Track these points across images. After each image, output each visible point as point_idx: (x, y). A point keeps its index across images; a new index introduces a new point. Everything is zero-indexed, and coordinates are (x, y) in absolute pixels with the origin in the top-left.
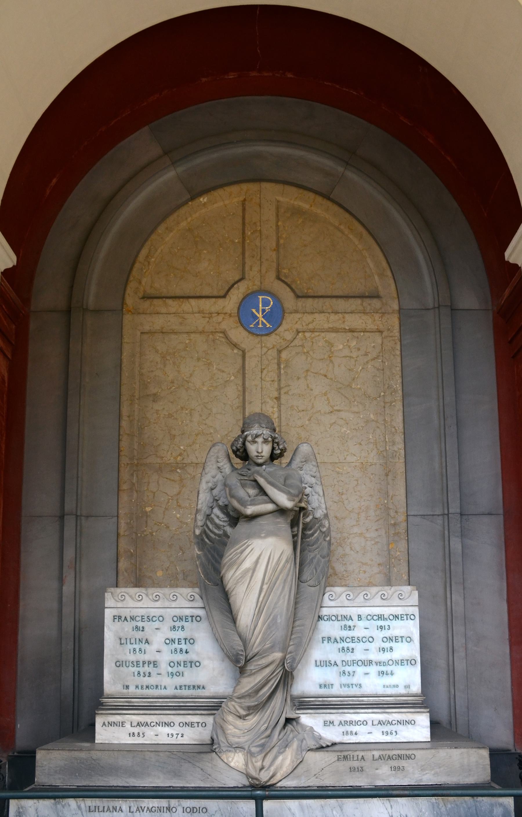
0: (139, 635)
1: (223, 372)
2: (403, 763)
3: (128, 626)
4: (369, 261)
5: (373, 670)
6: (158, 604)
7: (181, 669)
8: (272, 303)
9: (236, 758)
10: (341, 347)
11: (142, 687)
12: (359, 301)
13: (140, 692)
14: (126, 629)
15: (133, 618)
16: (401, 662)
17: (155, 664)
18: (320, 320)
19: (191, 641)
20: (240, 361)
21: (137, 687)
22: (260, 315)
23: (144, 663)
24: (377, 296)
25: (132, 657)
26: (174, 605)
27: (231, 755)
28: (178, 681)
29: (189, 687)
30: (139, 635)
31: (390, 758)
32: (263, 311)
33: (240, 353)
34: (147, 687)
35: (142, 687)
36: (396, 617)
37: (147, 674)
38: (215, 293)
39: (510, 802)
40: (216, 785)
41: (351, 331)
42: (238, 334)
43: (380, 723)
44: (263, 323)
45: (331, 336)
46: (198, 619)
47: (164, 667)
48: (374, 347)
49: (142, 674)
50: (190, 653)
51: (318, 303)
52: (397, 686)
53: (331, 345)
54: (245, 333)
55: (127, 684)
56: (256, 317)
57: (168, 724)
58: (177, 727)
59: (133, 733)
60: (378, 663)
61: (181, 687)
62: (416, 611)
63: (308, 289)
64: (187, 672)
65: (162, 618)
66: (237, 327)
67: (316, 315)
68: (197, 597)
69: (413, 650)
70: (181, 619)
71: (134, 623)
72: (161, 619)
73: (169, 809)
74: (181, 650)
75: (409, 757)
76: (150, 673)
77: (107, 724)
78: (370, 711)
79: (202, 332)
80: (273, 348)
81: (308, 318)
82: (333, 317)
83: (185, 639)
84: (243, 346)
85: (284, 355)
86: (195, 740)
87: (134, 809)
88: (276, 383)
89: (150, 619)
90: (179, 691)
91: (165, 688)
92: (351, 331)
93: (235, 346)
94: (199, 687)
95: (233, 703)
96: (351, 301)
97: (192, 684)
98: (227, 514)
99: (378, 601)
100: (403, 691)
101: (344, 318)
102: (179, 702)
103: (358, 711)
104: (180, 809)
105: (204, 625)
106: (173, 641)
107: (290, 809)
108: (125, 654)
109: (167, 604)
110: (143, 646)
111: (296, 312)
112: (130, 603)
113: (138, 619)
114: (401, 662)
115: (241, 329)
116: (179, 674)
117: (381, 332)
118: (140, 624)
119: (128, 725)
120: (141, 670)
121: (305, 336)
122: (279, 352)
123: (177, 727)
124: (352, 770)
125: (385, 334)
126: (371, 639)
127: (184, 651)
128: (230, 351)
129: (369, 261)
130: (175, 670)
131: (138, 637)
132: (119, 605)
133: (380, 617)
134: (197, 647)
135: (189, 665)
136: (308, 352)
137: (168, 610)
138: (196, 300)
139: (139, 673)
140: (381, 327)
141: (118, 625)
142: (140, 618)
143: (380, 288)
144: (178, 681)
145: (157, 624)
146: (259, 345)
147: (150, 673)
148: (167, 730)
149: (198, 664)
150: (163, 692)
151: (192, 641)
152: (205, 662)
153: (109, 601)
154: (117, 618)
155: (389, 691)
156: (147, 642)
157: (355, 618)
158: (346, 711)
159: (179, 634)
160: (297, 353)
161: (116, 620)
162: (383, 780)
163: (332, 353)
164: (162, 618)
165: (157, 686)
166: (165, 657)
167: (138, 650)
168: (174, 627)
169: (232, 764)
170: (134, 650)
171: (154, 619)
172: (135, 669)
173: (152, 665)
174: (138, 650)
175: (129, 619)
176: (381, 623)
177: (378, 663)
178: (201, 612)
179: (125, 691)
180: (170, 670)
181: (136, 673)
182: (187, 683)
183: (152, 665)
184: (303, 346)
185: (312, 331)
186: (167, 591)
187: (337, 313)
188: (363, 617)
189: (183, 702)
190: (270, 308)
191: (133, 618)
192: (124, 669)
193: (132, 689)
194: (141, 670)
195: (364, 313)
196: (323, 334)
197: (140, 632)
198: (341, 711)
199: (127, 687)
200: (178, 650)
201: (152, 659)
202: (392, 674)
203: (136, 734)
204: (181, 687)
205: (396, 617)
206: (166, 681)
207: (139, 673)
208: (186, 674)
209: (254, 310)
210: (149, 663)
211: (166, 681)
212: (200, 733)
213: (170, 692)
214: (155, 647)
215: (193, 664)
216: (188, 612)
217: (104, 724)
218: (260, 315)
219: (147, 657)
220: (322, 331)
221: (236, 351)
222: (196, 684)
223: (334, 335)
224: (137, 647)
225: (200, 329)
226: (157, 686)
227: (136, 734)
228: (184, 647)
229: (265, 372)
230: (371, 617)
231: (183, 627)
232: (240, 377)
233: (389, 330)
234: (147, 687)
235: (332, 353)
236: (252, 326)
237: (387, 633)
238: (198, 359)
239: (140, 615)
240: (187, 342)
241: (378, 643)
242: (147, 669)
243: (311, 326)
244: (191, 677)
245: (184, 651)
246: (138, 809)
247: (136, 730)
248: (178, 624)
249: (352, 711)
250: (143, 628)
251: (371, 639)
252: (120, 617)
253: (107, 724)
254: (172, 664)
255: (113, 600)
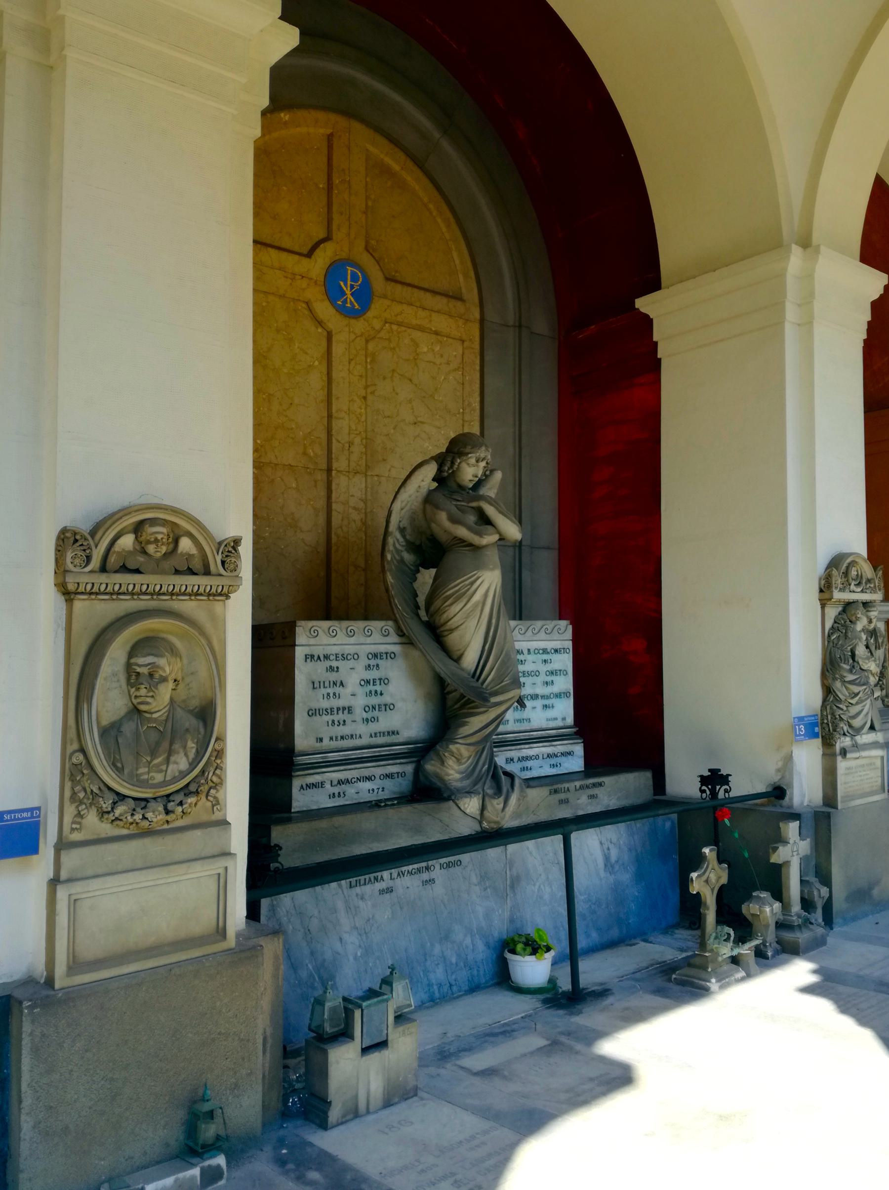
0: (333, 677)
1: (306, 353)
2: (596, 791)
3: (322, 666)
4: (455, 254)
5: (539, 703)
6: (352, 640)
7: (376, 713)
8: (361, 280)
9: (471, 804)
10: (425, 349)
11: (336, 738)
12: (445, 300)
13: (334, 744)
14: (319, 671)
15: (327, 657)
16: (558, 696)
17: (350, 710)
18: (409, 314)
19: (384, 681)
20: (324, 343)
21: (331, 738)
22: (348, 292)
23: (338, 709)
24: (458, 298)
25: (325, 704)
26: (369, 640)
27: (467, 800)
28: (374, 727)
29: (384, 733)
30: (333, 677)
31: (588, 787)
32: (352, 287)
33: (325, 333)
34: (342, 738)
35: (336, 738)
36: (556, 651)
37: (342, 723)
38: (297, 249)
39: (675, 816)
40: (454, 835)
41: (437, 333)
42: (324, 309)
43: (549, 756)
44: (351, 303)
45: (417, 334)
46: (393, 655)
47: (359, 714)
48: (455, 356)
49: (336, 723)
50: (384, 695)
51: (406, 292)
52: (556, 719)
53: (417, 345)
54: (332, 311)
55: (320, 736)
56: (343, 293)
57: (369, 779)
58: (378, 781)
59: (334, 794)
60: (543, 697)
61: (376, 734)
62: (569, 645)
63: (396, 272)
64: (382, 716)
65: (356, 656)
66: (323, 300)
67: (405, 306)
68: (392, 631)
69: (565, 683)
70: (375, 656)
71: (328, 663)
72: (356, 656)
73: (427, 868)
74: (376, 692)
75: (600, 785)
76: (344, 721)
77: (305, 787)
78: (541, 744)
79: (282, 297)
80: (361, 336)
81: (397, 308)
82: (422, 313)
83: (380, 679)
84: (330, 326)
85: (371, 346)
86: (395, 793)
87: (395, 875)
88: (364, 380)
89: (344, 657)
90: (374, 739)
91: (360, 737)
92: (437, 333)
93: (320, 323)
94: (393, 733)
95: (458, 746)
96: (438, 298)
97: (386, 730)
98: (404, 536)
99: (542, 635)
100: (560, 723)
101: (431, 316)
102: (375, 752)
103: (532, 745)
104: (438, 867)
105: (400, 662)
106: (368, 682)
107: (528, 848)
108: (318, 701)
109: (362, 639)
110: (338, 690)
111: (385, 297)
112: (324, 639)
113: (332, 657)
114: (558, 696)
115: (327, 303)
116: (375, 719)
117: (463, 341)
118: (334, 664)
119: (328, 785)
120: (336, 718)
121: (391, 328)
122: (367, 341)
123: (378, 781)
124: (561, 802)
125: (466, 344)
126: (537, 674)
127: (379, 692)
128: (313, 328)
129: (455, 254)
130: (369, 715)
131: (332, 679)
132: (312, 641)
133: (545, 651)
134: (391, 688)
135: (383, 708)
136: (394, 349)
137: (363, 646)
138: (277, 251)
139: (333, 721)
140: (464, 337)
141: (310, 664)
142: (334, 657)
143: (464, 290)
144: (374, 727)
145: (351, 663)
146: (347, 329)
147: (344, 721)
148: (368, 785)
149: (392, 707)
150: (358, 742)
151: (386, 681)
152: (399, 705)
153: (301, 637)
154: (310, 657)
155: (552, 724)
156: (342, 684)
157: (525, 652)
158: (522, 746)
159: (373, 674)
160: (384, 348)
161: (308, 660)
162: (583, 809)
163: (418, 354)
164: (356, 656)
165: (352, 736)
166: (360, 702)
167: (331, 695)
168: (369, 666)
169: (468, 811)
170: (328, 694)
171: (349, 657)
172: (329, 718)
173: (346, 712)
174: (331, 695)
175: (322, 658)
176: (545, 657)
177: (543, 697)
178: (396, 649)
179: (318, 744)
180: (365, 715)
181: (330, 723)
182: (382, 730)
183: (346, 712)
184: (389, 340)
185: (400, 324)
186: (361, 624)
187: (424, 309)
188: (532, 651)
189: (379, 752)
190: (360, 285)
191: (327, 657)
192: (317, 718)
193: (326, 741)
194: (336, 718)
195: (451, 316)
196: (409, 331)
197: (334, 674)
198: (519, 747)
199: (321, 740)
200: (373, 693)
201: (346, 704)
202: (553, 707)
203: (336, 795)
204: (376, 734)
205: (556, 651)
206: (363, 730)
207: (333, 721)
208: (380, 719)
209: (342, 284)
210: (344, 709)
211: (363, 730)
212: (400, 784)
213: (365, 741)
214: (349, 690)
215: (388, 707)
216: (382, 648)
217: (302, 787)
218: (348, 292)
219: (341, 703)
220: (410, 327)
221: (320, 330)
222: (390, 730)
223: (419, 334)
224: (331, 691)
225: (282, 292)
226: (352, 736)
227: (336, 795)
228: (378, 688)
229: (353, 363)
230: (537, 651)
231: (378, 665)
232: (325, 365)
233: (470, 340)
234: (342, 738)
235: (418, 354)
236: (339, 303)
237: (549, 667)
238: (278, 331)
239: (334, 653)
240: (264, 304)
241: (543, 677)
242: (341, 716)
243: (399, 319)
244: (386, 722)
245: (379, 692)
246: (399, 874)
247: (336, 790)
248: (373, 662)
249: (527, 746)
250: (338, 668)
251: (537, 674)
252: (312, 656)
253: (305, 787)
254: (367, 709)
255: (305, 637)
